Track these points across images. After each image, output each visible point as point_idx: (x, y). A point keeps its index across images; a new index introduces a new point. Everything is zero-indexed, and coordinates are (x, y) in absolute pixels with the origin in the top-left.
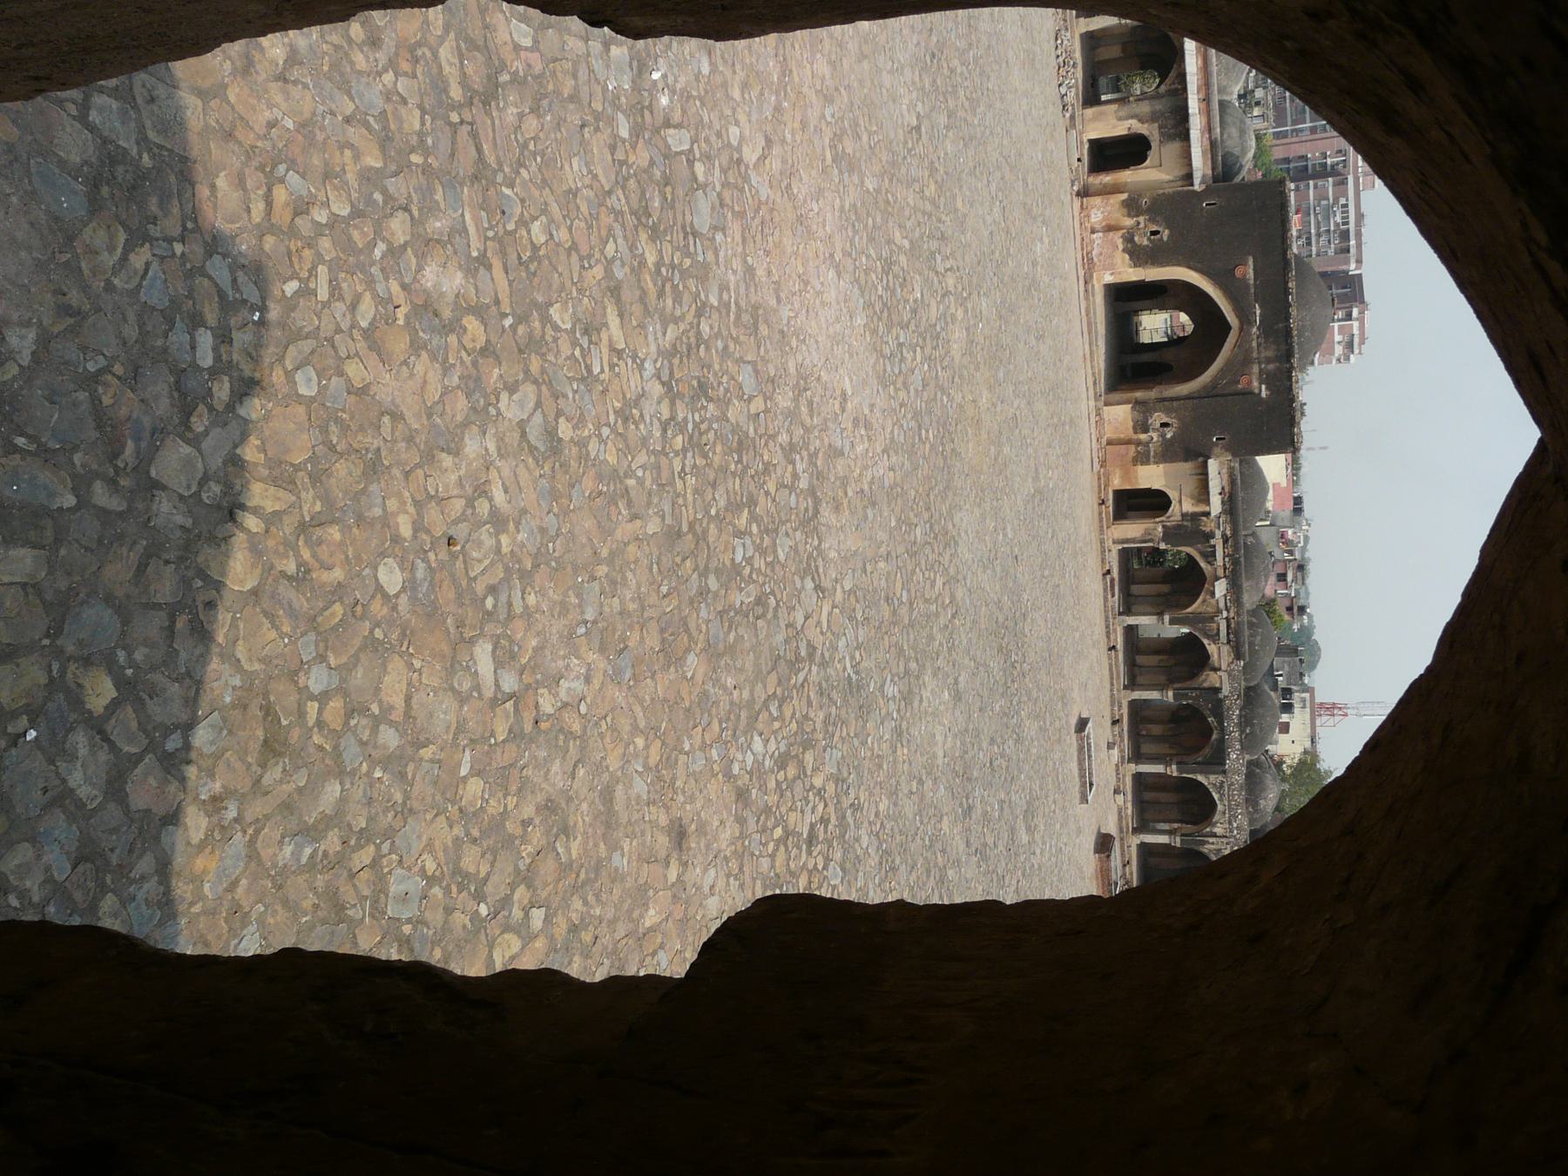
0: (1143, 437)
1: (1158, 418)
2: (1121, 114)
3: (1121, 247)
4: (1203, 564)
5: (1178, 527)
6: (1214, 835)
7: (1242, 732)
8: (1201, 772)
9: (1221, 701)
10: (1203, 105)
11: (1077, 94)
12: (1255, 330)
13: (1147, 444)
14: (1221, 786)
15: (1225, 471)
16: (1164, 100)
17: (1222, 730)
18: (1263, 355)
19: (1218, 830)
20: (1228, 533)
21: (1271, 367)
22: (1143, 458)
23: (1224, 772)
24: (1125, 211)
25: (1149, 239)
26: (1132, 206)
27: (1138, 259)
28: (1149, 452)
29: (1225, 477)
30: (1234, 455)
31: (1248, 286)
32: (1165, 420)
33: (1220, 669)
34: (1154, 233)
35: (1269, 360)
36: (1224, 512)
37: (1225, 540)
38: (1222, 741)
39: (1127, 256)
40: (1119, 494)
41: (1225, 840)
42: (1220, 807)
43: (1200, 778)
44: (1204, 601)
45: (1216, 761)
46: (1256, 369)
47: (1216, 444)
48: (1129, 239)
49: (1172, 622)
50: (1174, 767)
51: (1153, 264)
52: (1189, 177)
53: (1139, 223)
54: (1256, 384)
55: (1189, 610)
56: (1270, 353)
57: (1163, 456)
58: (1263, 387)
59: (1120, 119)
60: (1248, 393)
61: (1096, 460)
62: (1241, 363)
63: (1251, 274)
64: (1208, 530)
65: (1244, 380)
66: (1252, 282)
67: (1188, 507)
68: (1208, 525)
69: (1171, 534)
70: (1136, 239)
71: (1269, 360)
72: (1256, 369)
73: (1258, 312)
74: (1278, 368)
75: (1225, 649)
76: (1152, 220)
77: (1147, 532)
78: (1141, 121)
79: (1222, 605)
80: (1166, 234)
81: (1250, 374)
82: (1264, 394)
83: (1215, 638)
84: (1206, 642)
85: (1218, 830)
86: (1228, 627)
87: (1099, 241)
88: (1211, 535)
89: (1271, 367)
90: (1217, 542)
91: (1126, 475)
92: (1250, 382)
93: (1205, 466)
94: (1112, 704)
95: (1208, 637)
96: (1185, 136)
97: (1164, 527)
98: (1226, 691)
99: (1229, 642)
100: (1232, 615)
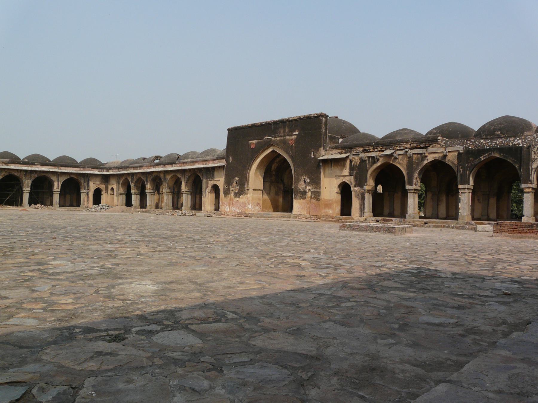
0: (309, 194)
3: (238, 199)
4: (379, 164)
5: (356, 178)
7: (499, 137)
10: (207, 163)
11: (198, 212)
12: (273, 139)
15: (331, 152)
17: (492, 150)
18: (282, 134)
20: (362, 149)
21: (287, 130)
22: (317, 195)
23: (529, 147)
24: (228, 196)
27: (242, 191)
28: (315, 192)
29: (334, 151)
31: (258, 143)
35: (284, 132)
37: (365, 151)
38: (501, 150)
39: (241, 196)
44: (400, 164)
46: (287, 138)
49: (411, 184)
50: (523, 186)
53: (232, 190)
54: (293, 137)
55: (404, 172)
56: (282, 131)
58: (294, 133)
60: (297, 141)
61: (315, 220)
62: (284, 144)
63: (254, 141)
64: (359, 161)
65: (290, 143)
66: (257, 141)
67: (346, 172)
68: (356, 160)
70: (236, 192)
71: (284, 132)
73: (267, 137)
74: (288, 127)
75: (430, 149)
76: (232, 184)
77: (357, 196)
78: (207, 187)
79: (401, 152)
80: (237, 178)
81: (289, 140)
82: (297, 133)
83: (423, 157)
84: (425, 162)
86: (416, 148)
87: (235, 208)
88: (362, 161)
89: (287, 130)
90: (364, 156)
91: (328, 205)
93: (325, 161)
94: (465, 229)
95: (423, 160)
96: (213, 168)
97: (355, 186)
100: (408, 146)
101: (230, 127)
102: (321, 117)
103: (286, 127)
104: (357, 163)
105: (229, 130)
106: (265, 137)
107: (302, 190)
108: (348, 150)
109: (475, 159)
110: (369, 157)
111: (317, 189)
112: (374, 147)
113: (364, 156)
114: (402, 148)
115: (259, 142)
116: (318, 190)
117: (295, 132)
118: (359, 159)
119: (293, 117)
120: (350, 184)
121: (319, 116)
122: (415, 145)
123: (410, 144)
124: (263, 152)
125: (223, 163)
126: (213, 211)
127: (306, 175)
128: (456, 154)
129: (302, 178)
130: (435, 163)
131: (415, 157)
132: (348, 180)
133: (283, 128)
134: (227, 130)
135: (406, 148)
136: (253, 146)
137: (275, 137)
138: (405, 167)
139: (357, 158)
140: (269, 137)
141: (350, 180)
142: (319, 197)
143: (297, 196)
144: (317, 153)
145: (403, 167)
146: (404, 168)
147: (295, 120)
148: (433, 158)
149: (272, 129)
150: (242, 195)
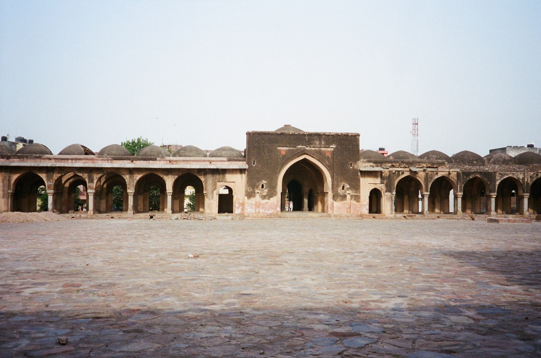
0: (348, 197)
1: (340, 191)
2: (210, 197)
4: (403, 176)
5: (387, 186)
6: (523, 179)
8: (495, 183)
9: (463, 173)
12: (307, 148)
13: (352, 196)
14: (501, 174)
16: (208, 179)
19: (521, 177)
20: (390, 165)
21: (323, 143)
25: (265, 189)
26: (250, 195)
27: (273, 194)
28: (355, 195)
30: (359, 160)
31: (289, 150)
32: (341, 188)
33: (449, 172)
34: (263, 186)
35: (320, 144)
36: (381, 166)
37: (393, 166)
38: (480, 173)
40: (371, 211)
41: (526, 174)
42: (511, 175)
43: (498, 183)
45: (490, 176)
46: (323, 149)
47: (353, 167)
48: (264, 197)
51: (276, 188)
52: (242, 171)
54: (329, 149)
55: (423, 183)
56: (318, 143)
57: (357, 189)
58: (331, 146)
59: (213, 198)
60: (333, 153)
64: (388, 173)
66: (288, 148)
69: (389, 190)
70: (264, 194)
71: (320, 144)
72: (323, 149)
75: (440, 169)
76: (257, 187)
80: (264, 182)
81: (325, 152)
82: (334, 147)
84: (436, 177)
85: (521, 177)
86: (430, 167)
89: (323, 143)
90: (394, 169)
92: (328, 151)
93: (362, 172)
97: (386, 192)
98: (458, 170)
99: (436, 167)
100: (425, 165)
101: (250, 130)
102: (357, 137)
103: (322, 140)
104: (387, 174)
105: (248, 134)
106: (299, 145)
107: (342, 194)
108: (379, 165)
109: (467, 177)
110: (396, 171)
111: (357, 193)
112: (400, 164)
113: (394, 169)
114: (421, 167)
115: (291, 149)
116: (358, 194)
117: (332, 145)
118: (389, 172)
119: (330, 133)
120: (381, 190)
121: (357, 136)
122: (430, 165)
123: (427, 165)
124: (292, 160)
125: (243, 165)
126: (217, 214)
127: (345, 182)
128: (456, 173)
129: (342, 184)
130: (443, 178)
131: (430, 173)
132: (379, 187)
133: (319, 141)
134: (247, 134)
135: (424, 167)
136: (283, 153)
137: (311, 147)
138: (423, 180)
139: (387, 171)
140: (303, 147)
141: (381, 187)
142: (359, 200)
143: (337, 199)
144: (355, 165)
145: (422, 179)
146: (423, 180)
147: (332, 135)
148: (441, 175)
149: (306, 140)
150: (273, 197)
